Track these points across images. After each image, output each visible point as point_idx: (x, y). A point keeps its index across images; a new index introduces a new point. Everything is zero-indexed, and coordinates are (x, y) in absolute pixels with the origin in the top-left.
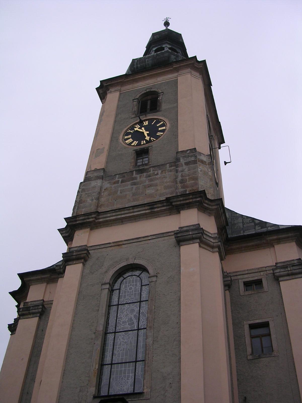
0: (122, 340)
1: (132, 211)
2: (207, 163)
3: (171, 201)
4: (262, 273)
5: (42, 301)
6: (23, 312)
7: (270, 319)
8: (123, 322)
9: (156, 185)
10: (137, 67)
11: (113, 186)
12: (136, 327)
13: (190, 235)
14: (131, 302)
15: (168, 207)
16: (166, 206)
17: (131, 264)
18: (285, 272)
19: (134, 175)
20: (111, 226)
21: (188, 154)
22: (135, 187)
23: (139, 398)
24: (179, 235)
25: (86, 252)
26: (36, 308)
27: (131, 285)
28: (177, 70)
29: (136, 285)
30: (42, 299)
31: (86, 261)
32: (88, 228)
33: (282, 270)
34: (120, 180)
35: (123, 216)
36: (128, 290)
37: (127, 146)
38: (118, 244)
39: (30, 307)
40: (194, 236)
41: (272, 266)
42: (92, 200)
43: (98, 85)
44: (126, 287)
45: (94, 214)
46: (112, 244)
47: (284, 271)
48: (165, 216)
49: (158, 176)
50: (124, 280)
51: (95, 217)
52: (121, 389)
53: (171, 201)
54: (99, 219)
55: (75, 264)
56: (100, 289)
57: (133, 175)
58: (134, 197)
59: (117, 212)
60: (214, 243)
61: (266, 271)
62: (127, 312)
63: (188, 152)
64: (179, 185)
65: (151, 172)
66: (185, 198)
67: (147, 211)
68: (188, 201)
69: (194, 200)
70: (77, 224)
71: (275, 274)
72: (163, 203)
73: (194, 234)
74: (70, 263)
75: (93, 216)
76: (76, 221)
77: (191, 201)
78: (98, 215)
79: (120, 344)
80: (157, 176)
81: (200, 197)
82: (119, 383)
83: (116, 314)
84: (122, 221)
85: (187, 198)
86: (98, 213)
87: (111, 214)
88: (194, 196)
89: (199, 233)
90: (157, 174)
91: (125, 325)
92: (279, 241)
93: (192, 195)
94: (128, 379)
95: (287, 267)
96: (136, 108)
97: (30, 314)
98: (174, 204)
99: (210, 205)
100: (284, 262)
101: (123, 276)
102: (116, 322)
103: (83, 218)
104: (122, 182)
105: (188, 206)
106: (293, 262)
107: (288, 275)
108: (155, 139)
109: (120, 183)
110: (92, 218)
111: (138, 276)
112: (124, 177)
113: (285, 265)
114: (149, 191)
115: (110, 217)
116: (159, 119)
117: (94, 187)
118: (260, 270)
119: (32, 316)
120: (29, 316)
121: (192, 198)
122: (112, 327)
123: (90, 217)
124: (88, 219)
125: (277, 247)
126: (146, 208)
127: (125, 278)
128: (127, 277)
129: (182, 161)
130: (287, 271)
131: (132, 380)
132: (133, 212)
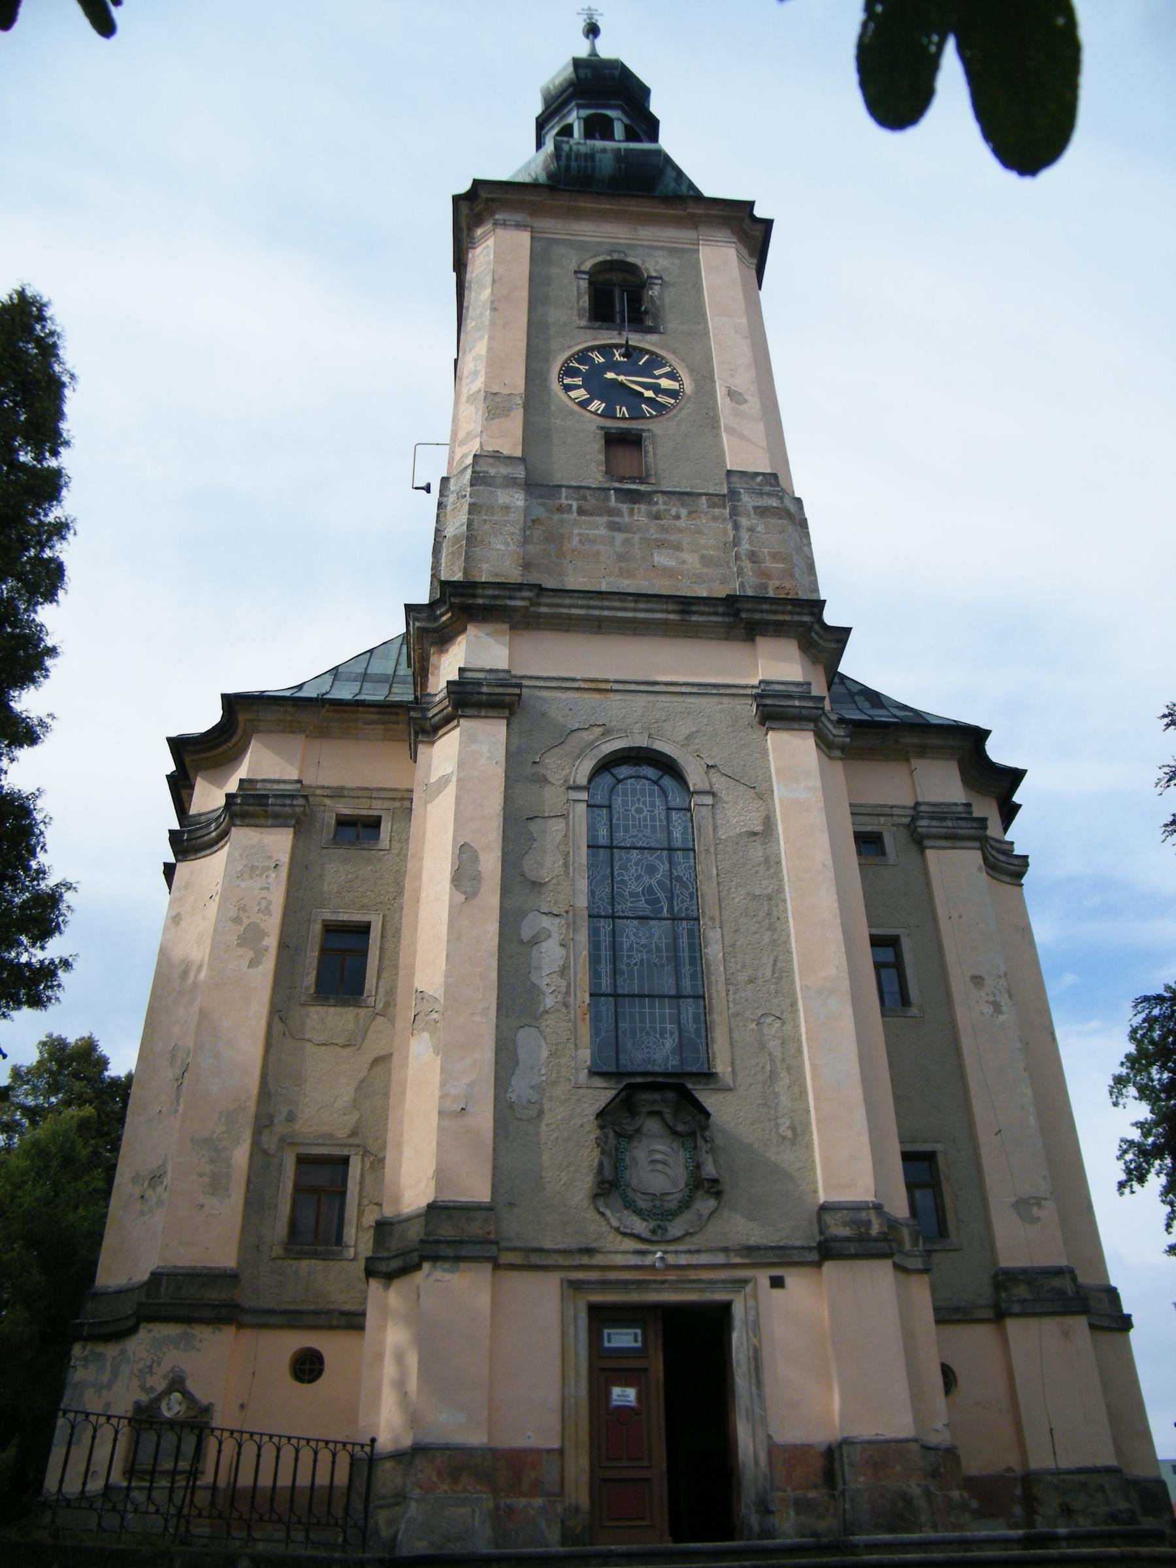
0: (633, 938)
1: (632, 605)
2: (797, 521)
3: (739, 605)
4: (882, 819)
5: (299, 786)
6: (245, 808)
7: (902, 930)
8: (632, 894)
9: (678, 547)
10: (568, 168)
12: (665, 910)
13: (795, 707)
14: (645, 845)
15: (727, 619)
16: (724, 614)
17: (639, 749)
18: (940, 830)
19: (613, 501)
20: (567, 631)
21: (759, 485)
22: (619, 537)
23: (707, 1084)
24: (768, 702)
25: (517, 691)
26: (288, 802)
27: (639, 800)
29: (653, 804)
30: (296, 778)
31: (512, 714)
32: (504, 622)
33: (935, 823)
34: (575, 505)
35: (606, 613)
36: (633, 812)
37: (576, 408)
38: (598, 687)
39: (267, 796)
40: (804, 712)
41: (904, 807)
43: (464, 187)
44: (625, 803)
45: (531, 590)
46: (583, 685)
47: (939, 827)
48: (712, 639)
49: (681, 523)
50: (620, 786)
51: (530, 599)
52: (649, 1059)
53: (739, 605)
54: (539, 605)
55: (485, 717)
56: (563, 799)
57: (608, 499)
58: (623, 565)
59: (591, 598)
60: (835, 736)
61: (892, 815)
62: (637, 870)
63: (759, 479)
64: (747, 565)
66: (774, 607)
67: (672, 617)
68: (780, 617)
69: (796, 618)
70: (479, 605)
71: (919, 830)
72: (715, 605)
73: (804, 707)
74: (469, 712)
76: (474, 596)
77: (788, 618)
78: (538, 596)
79: (631, 949)
80: (677, 523)
81: (812, 614)
82: (643, 1043)
83: (609, 870)
84: (598, 626)
85: (780, 608)
86: (540, 589)
87: (574, 601)
88: (797, 610)
89: (817, 708)
90: (678, 517)
91: (636, 901)
92: (923, 752)
93: (793, 605)
94: (662, 1036)
95: (945, 819)
96: (586, 298)
97: (266, 815)
98: (744, 615)
99: (821, 638)
100: (935, 805)
101: (612, 770)
102: (613, 889)
103: (497, 593)
105: (778, 630)
106: (954, 809)
107: (945, 837)
108: (654, 413)
109: (575, 514)
110: (523, 599)
111: (656, 783)
112: (585, 499)
113: (941, 812)
114: (662, 559)
115: (569, 606)
116: (658, 356)
117: (506, 508)
118: (878, 811)
119: (270, 822)
120: (263, 821)
121: (791, 613)
122: (603, 901)
123: (518, 594)
124: (511, 598)
125: (915, 763)
126: (670, 607)
127: (619, 781)
128: (625, 779)
129: (748, 501)
130: (944, 827)
131: (674, 1040)
132: (635, 610)
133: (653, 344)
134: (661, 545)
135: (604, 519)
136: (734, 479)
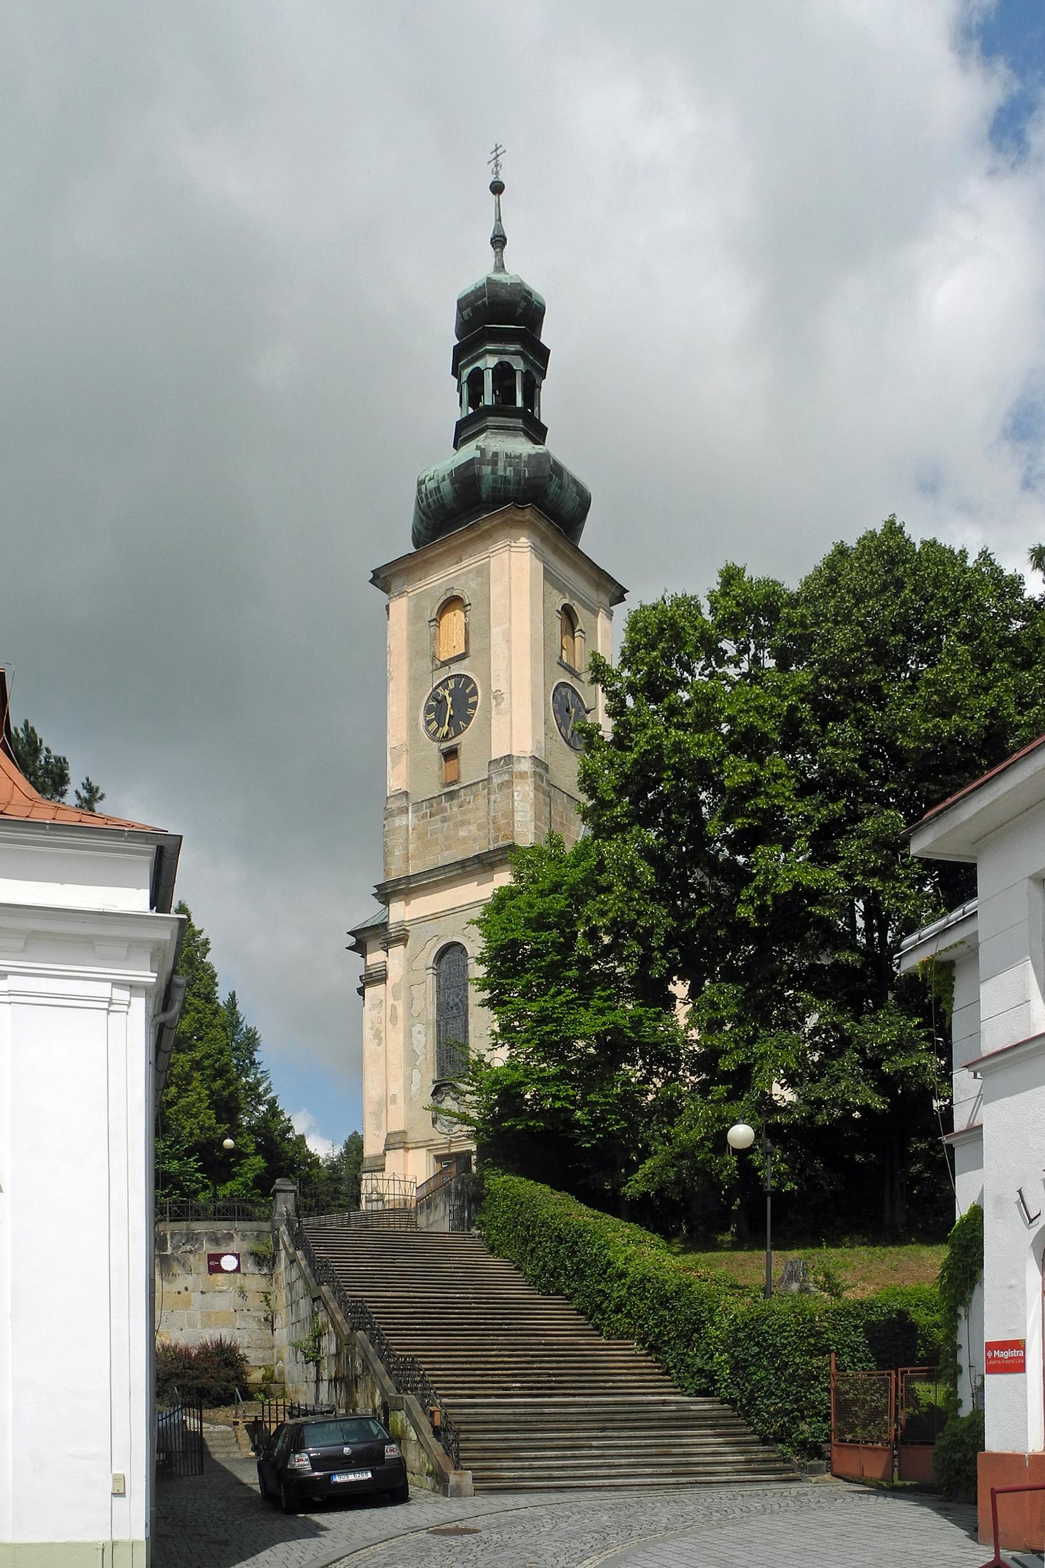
11: (421, 823)
22: (446, 824)
28: (487, 536)
42: (400, 851)
49: (471, 806)
54: (411, 883)
65: (463, 798)
75: (403, 881)
80: (469, 807)
104: (431, 816)
112: (432, 806)
114: (462, 833)
133: (466, 669)
134: (463, 823)
135: (438, 817)
136: (492, 767)
